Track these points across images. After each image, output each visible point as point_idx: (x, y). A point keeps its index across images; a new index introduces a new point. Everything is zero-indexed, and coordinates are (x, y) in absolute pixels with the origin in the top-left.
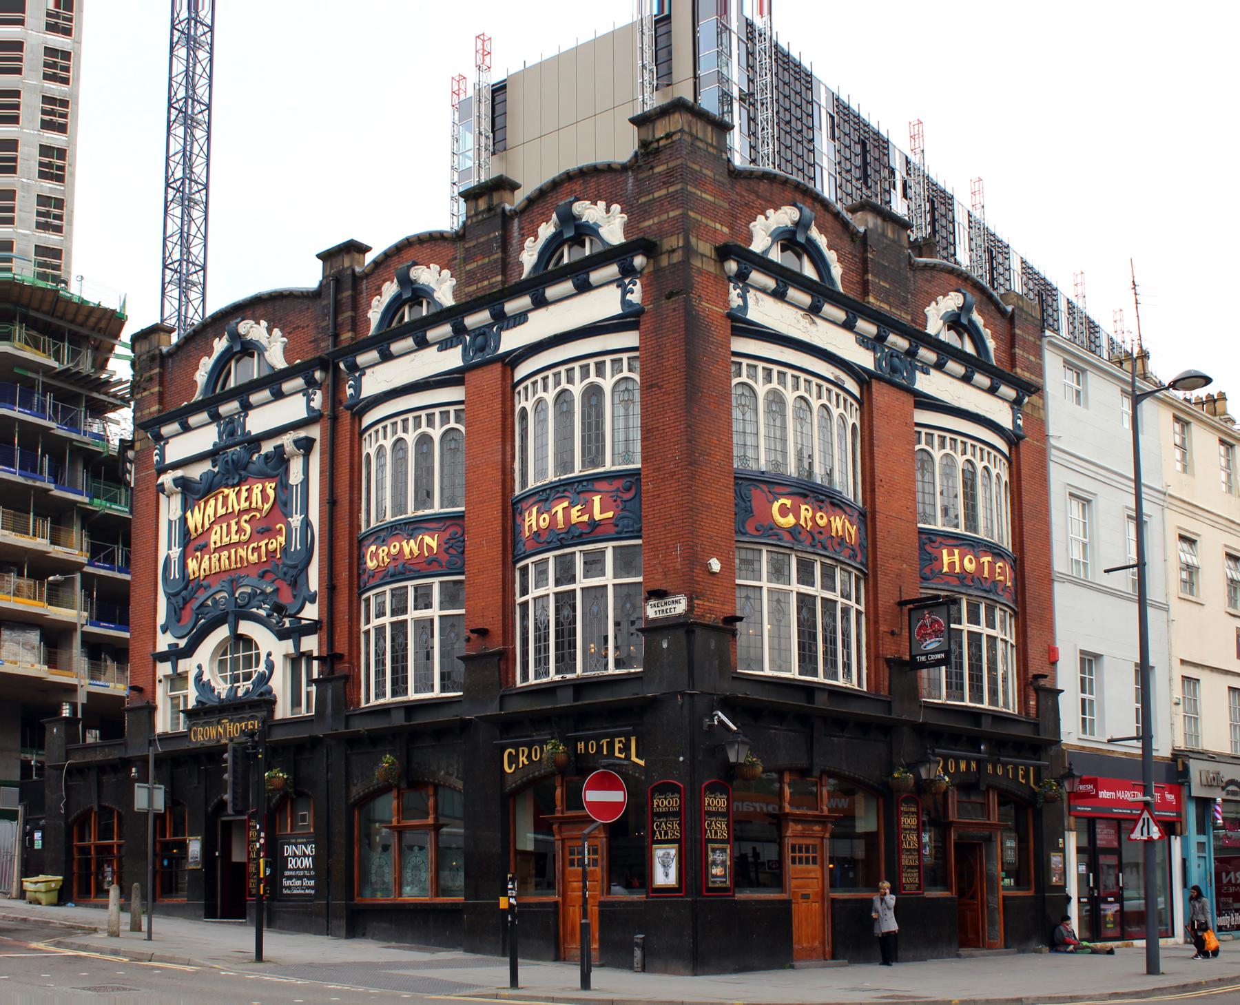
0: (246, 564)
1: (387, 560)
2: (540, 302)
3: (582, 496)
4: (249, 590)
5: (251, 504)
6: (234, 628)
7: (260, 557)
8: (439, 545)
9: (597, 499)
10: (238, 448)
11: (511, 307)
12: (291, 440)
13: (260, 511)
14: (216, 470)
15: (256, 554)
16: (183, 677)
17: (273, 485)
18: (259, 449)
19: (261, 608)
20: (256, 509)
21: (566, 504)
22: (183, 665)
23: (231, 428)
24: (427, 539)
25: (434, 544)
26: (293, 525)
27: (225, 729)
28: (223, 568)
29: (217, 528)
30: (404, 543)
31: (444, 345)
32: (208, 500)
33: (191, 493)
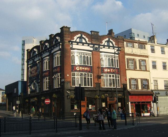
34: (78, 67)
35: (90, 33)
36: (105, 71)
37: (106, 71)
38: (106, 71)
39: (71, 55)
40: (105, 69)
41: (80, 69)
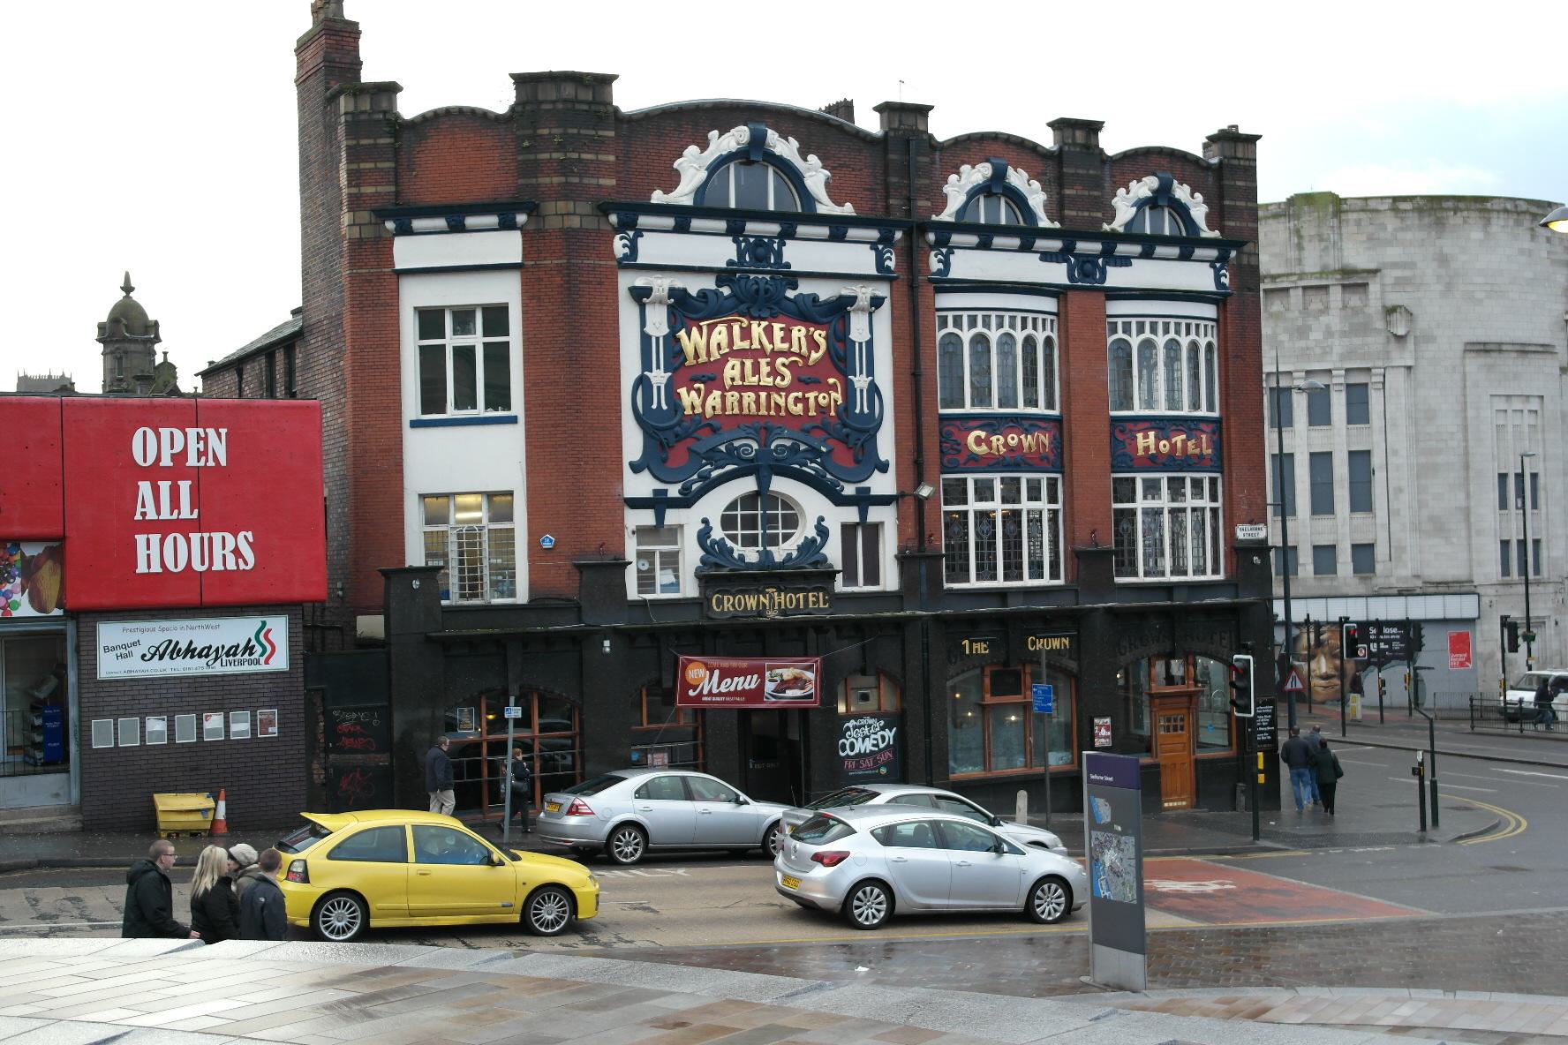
0: (783, 413)
1: (1003, 450)
2: (1147, 255)
3: (1194, 433)
4: (788, 443)
5: (791, 346)
6: (763, 483)
7: (806, 409)
8: (1051, 443)
9: (1204, 437)
10: (768, 277)
11: (1122, 249)
12: (860, 296)
13: (806, 358)
14: (726, 291)
15: (800, 406)
16: (676, 531)
17: (824, 333)
18: (795, 287)
19: (806, 466)
20: (799, 355)
21: (1184, 437)
22: (672, 517)
23: (760, 251)
24: (1042, 437)
25: (1047, 442)
26: (857, 385)
27: (771, 598)
28: (746, 411)
29: (732, 362)
30: (1022, 437)
31: (1047, 256)
32: (715, 325)
33: (684, 309)
34: (983, 434)
35: (1047, 140)
36: (1141, 452)
37: (1147, 449)
38: (1147, 449)
39: (940, 334)
40: (1140, 436)
41: (993, 451)
